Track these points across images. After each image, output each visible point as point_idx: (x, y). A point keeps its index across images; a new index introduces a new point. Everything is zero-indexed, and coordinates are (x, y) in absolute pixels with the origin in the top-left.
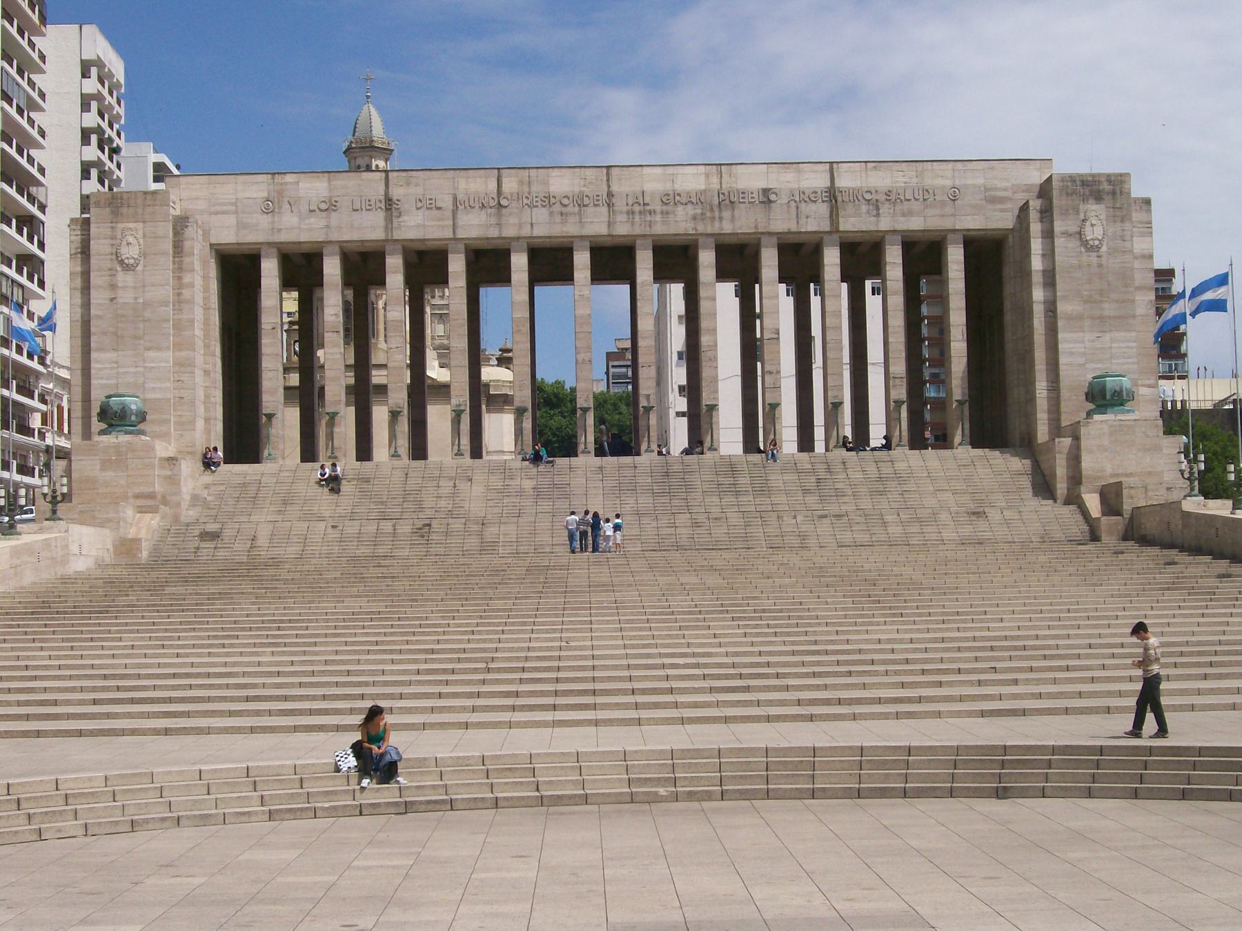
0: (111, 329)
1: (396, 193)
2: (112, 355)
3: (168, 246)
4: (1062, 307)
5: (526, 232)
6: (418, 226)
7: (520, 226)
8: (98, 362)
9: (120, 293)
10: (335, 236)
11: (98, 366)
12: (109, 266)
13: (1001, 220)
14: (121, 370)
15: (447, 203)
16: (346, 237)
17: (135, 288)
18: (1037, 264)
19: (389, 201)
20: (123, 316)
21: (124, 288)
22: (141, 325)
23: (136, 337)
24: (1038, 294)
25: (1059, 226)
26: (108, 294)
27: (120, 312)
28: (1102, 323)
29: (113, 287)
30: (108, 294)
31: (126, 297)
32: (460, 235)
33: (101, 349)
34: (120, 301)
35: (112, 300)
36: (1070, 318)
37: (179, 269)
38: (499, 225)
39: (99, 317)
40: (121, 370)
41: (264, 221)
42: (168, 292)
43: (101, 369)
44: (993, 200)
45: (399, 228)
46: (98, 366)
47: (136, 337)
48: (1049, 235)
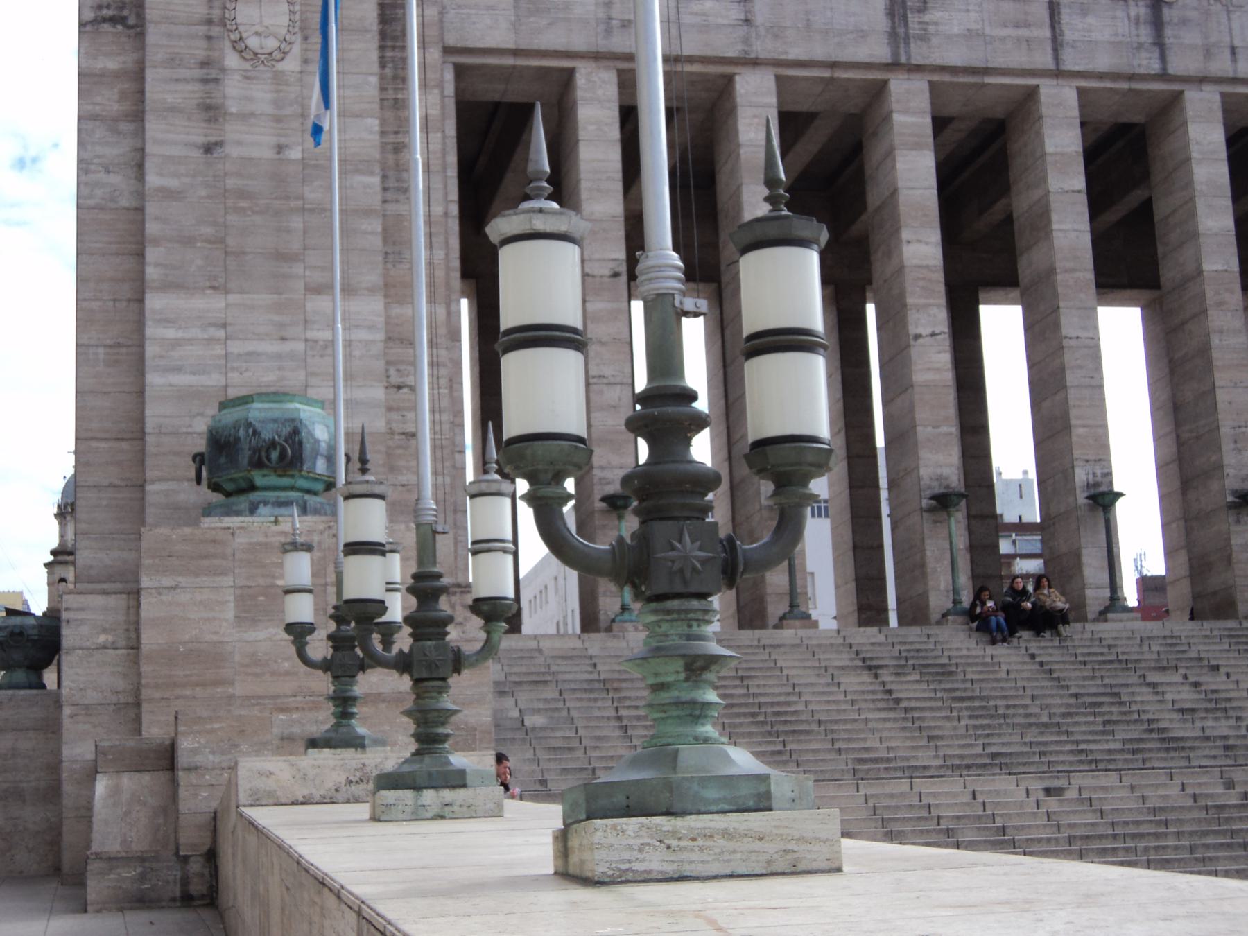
0: (208, 230)
2: (214, 304)
5: (1221, 65)
6: (970, 35)
7: (1208, 53)
8: (166, 321)
9: (232, 131)
10: (763, 48)
11: (171, 333)
12: (201, 54)
14: (235, 347)
16: (795, 53)
17: (278, 119)
20: (242, 194)
21: (244, 117)
22: (297, 223)
23: (282, 257)
26: (199, 134)
27: (231, 182)
29: (211, 111)
30: (199, 134)
31: (250, 143)
32: (1071, 61)
33: (167, 286)
34: (233, 151)
35: (208, 149)
38: (1160, 44)
39: (168, 194)
40: (235, 347)
43: (176, 343)
45: (924, 37)
46: (171, 333)
47: (282, 257)
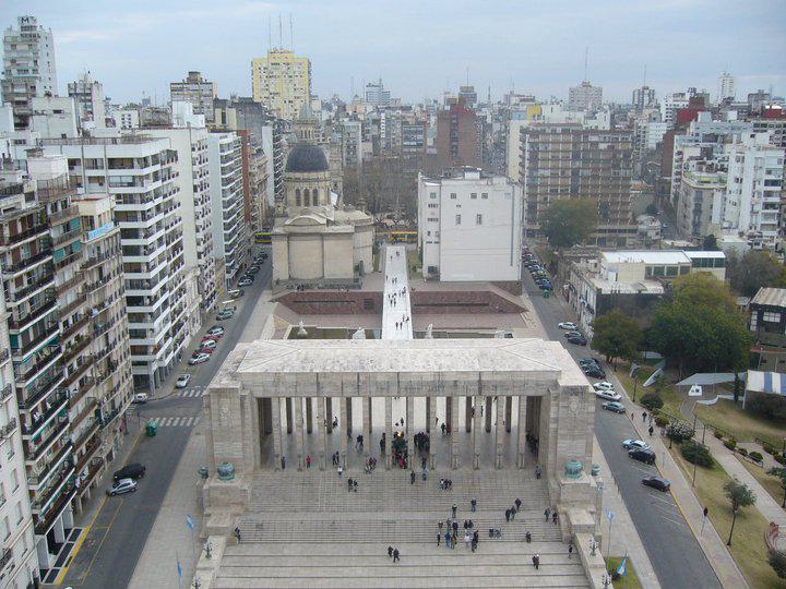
1: (321, 380)
3: (239, 407)
4: (559, 432)
13: (540, 392)
15: (339, 384)
18: (552, 415)
19: (318, 383)
24: (552, 426)
25: (561, 404)
28: (574, 437)
29: (220, 420)
31: (224, 424)
36: (562, 435)
37: (243, 414)
41: (273, 389)
42: (239, 423)
44: (537, 385)
48: (557, 405)
